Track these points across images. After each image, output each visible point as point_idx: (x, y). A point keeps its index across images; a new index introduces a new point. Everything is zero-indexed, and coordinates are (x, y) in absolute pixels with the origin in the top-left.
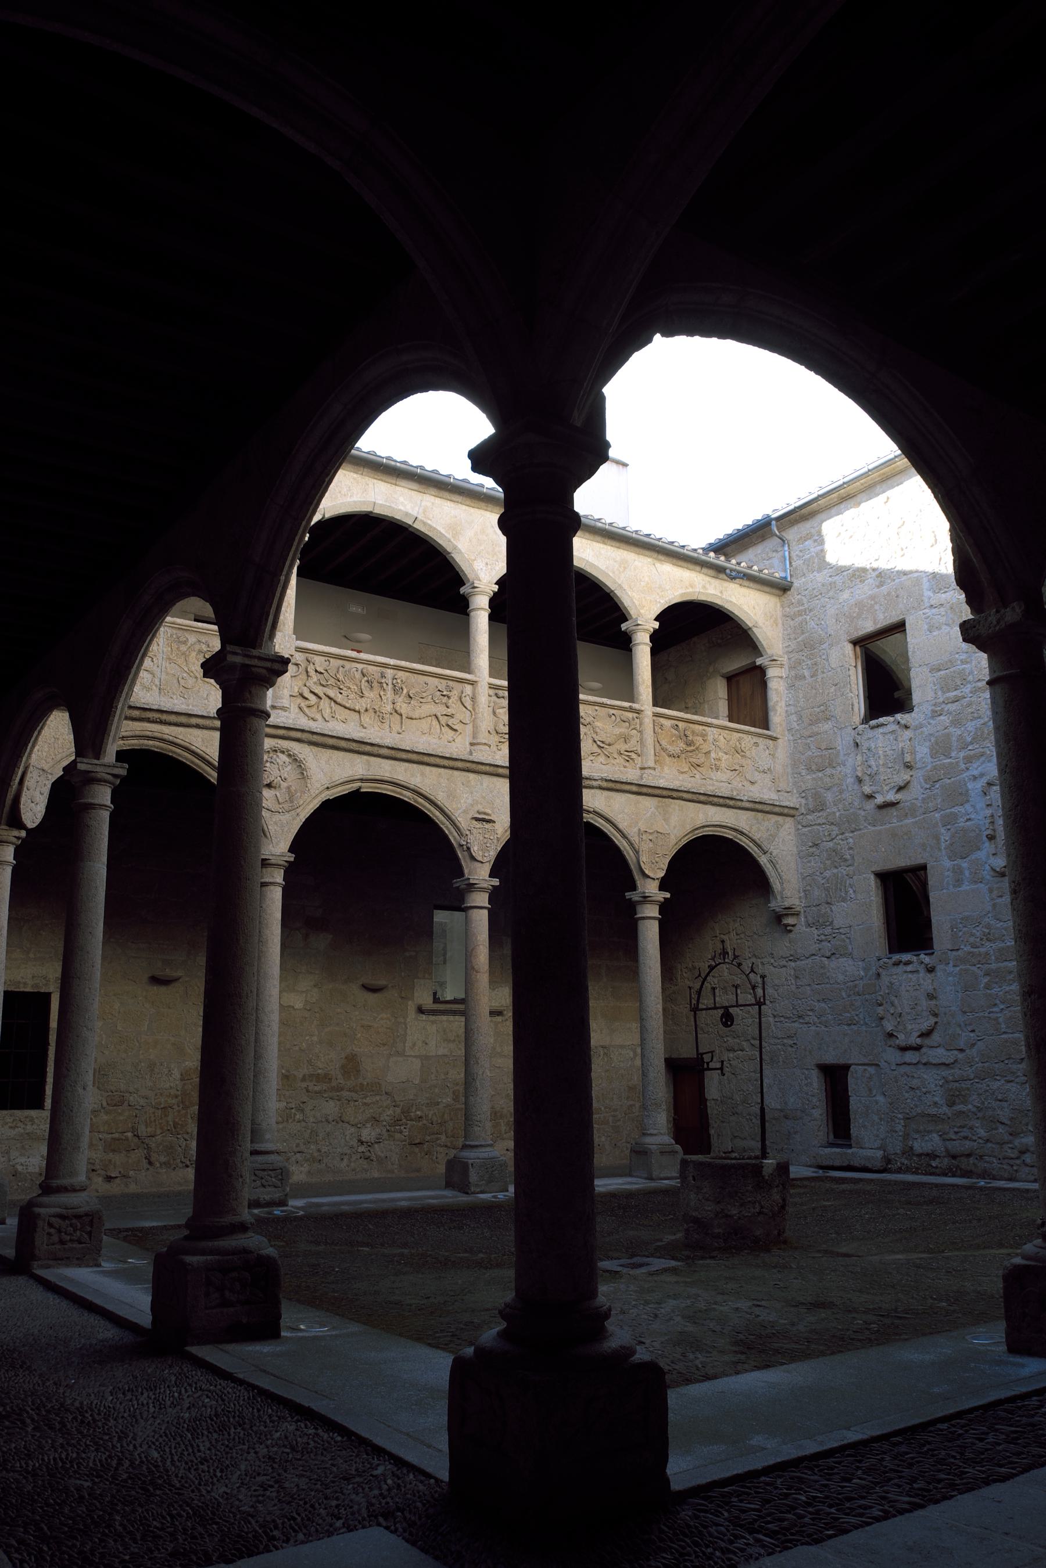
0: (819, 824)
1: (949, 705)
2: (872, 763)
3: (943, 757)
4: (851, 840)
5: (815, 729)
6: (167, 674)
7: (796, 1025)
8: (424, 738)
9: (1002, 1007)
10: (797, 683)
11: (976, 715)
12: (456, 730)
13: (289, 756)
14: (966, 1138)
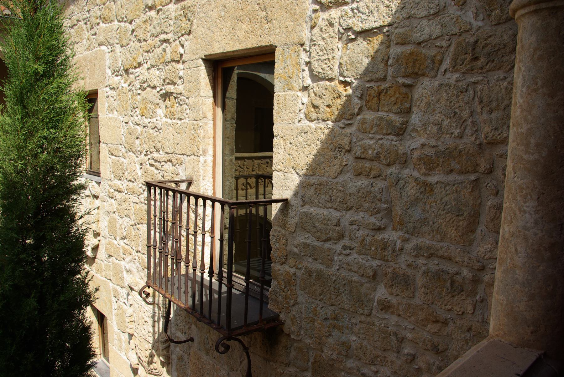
3: (113, 237)
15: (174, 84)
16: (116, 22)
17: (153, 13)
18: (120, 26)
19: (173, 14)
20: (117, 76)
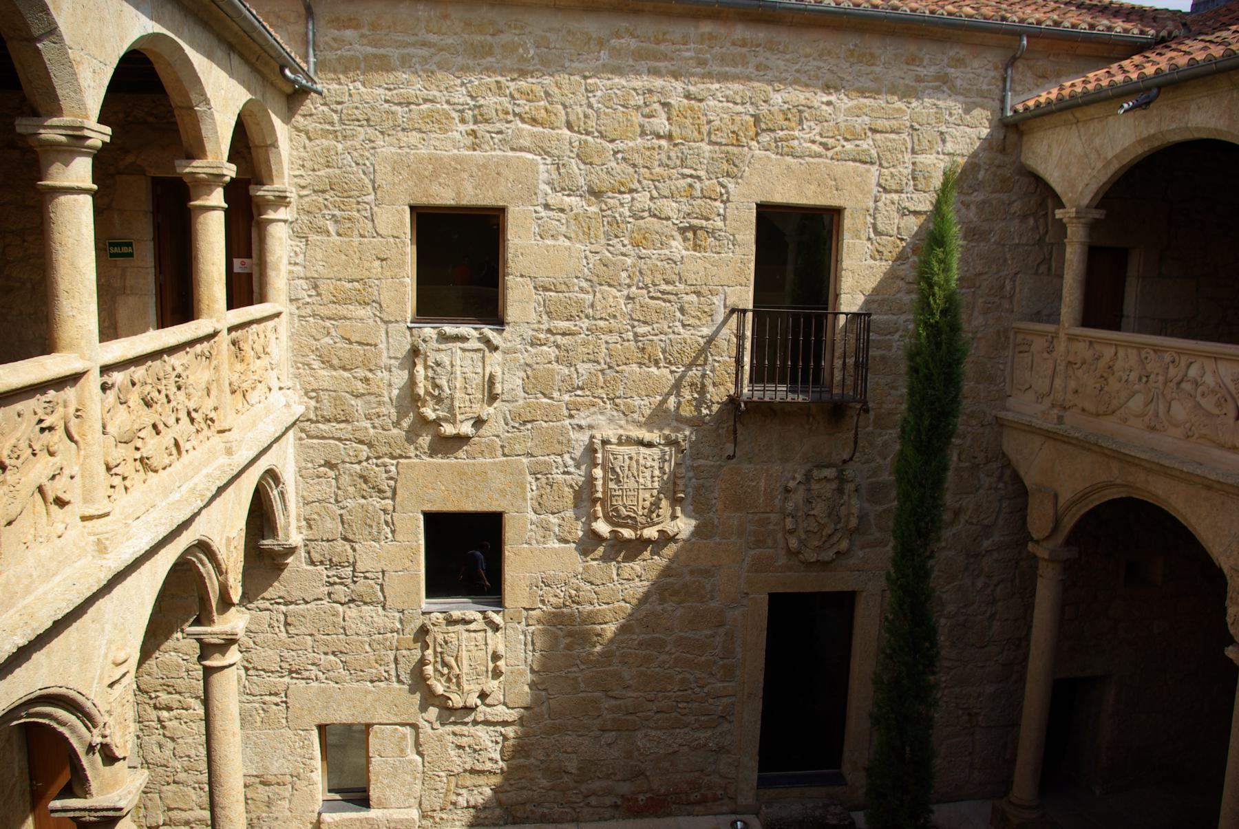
0: (339, 439)
1: (559, 338)
2: (443, 382)
3: (539, 395)
4: (393, 468)
5: (342, 310)
7: (287, 679)
9: (582, 667)
10: (313, 237)
11: (591, 357)
14: (523, 788)
15: (708, 219)
16: (568, 133)
17: (663, 143)
18: (586, 142)
19: (707, 155)
20: (569, 195)
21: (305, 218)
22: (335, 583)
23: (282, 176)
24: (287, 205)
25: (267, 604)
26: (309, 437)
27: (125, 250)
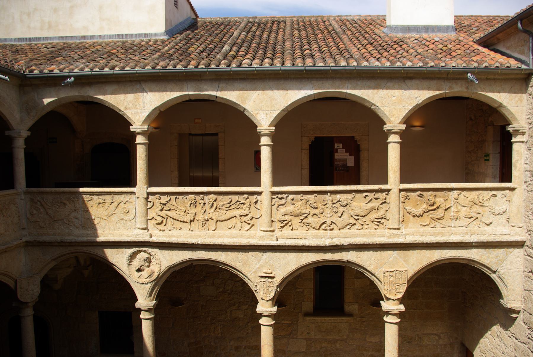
6: (85, 218)
8: (230, 231)
12: (249, 224)
13: (149, 253)
21: (530, 139)
22: (529, 338)
23: (515, 119)
24: (523, 134)
25: (510, 335)
26: (529, 256)
27: (487, 158)
